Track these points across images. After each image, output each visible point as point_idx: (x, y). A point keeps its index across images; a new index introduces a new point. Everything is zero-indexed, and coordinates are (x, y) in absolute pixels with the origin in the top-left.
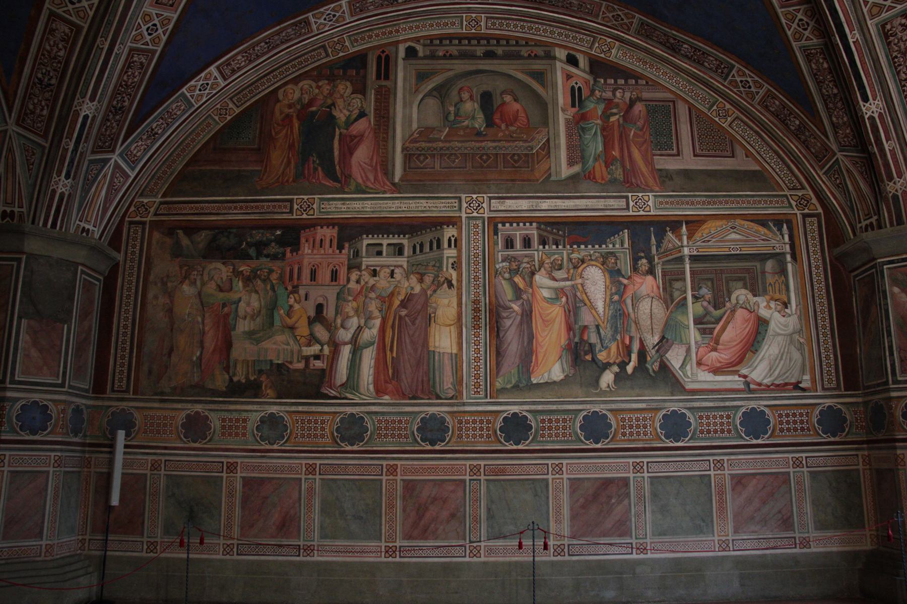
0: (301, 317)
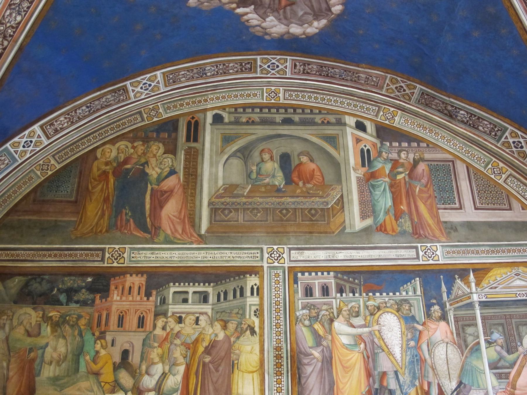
0: (107, 363)
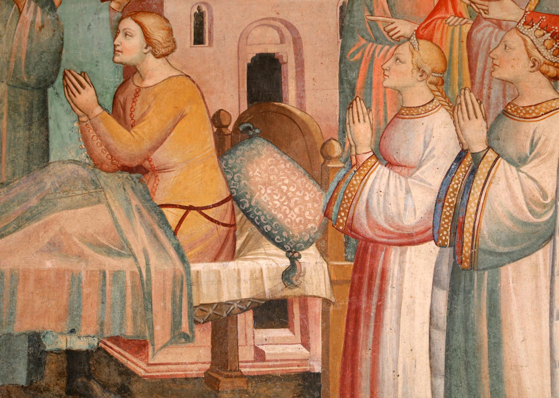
0: (182, 117)
